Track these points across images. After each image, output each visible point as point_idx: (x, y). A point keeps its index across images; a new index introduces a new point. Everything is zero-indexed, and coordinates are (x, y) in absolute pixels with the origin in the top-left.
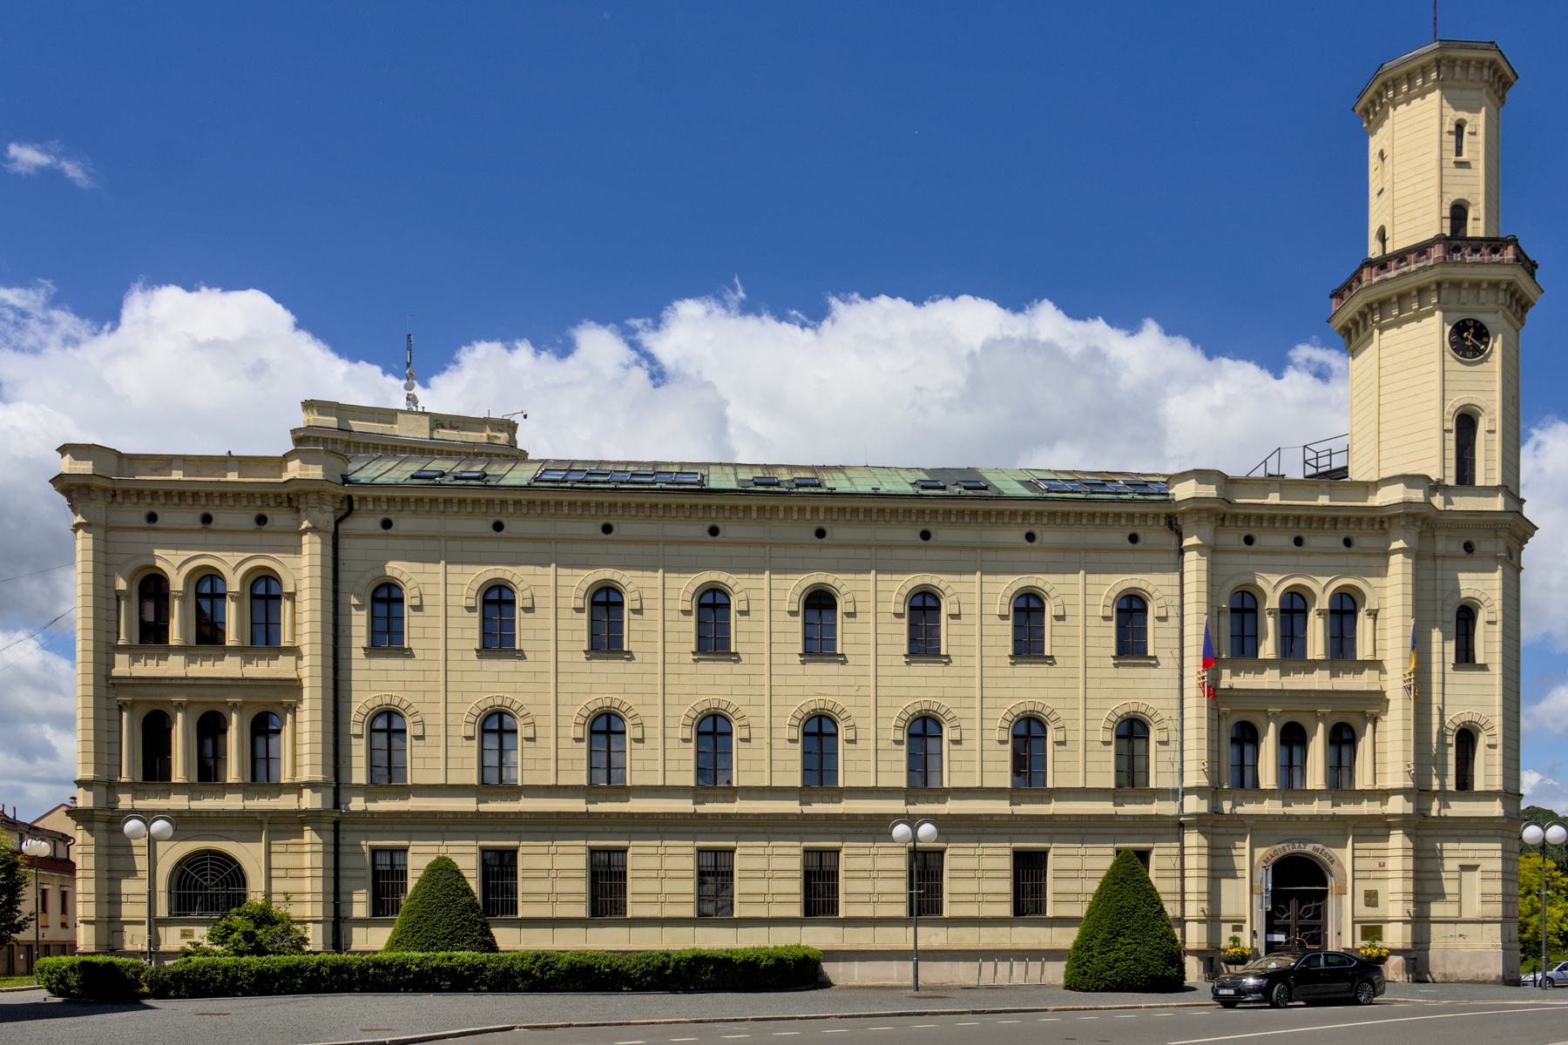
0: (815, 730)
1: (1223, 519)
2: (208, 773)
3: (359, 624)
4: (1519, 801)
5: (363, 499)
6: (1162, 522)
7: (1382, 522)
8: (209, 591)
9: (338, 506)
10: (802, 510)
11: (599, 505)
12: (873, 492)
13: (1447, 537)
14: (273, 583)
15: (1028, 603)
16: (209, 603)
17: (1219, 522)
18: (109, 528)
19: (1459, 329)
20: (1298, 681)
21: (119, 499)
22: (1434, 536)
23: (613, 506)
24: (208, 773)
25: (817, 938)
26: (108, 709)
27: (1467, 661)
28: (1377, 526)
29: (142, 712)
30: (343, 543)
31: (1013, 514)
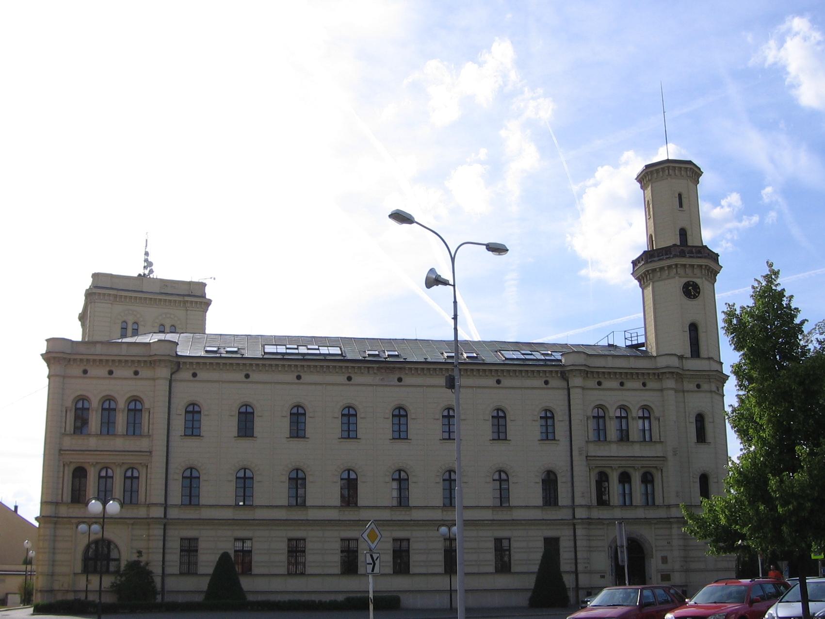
0: (397, 477)
1: (587, 374)
3: (179, 424)
5: (185, 363)
6: (559, 375)
7: (658, 376)
8: (108, 407)
9: (173, 366)
12: (424, 360)
13: (688, 382)
14: (138, 403)
15: (498, 413)
17: (585, 375)
18: (64, 377)
20: (624, 451)
21: (72, 363)
22: (683, 382)
25: (399, 583)
28: (656, 377)
29: (72, 467)
30: (173, 384)
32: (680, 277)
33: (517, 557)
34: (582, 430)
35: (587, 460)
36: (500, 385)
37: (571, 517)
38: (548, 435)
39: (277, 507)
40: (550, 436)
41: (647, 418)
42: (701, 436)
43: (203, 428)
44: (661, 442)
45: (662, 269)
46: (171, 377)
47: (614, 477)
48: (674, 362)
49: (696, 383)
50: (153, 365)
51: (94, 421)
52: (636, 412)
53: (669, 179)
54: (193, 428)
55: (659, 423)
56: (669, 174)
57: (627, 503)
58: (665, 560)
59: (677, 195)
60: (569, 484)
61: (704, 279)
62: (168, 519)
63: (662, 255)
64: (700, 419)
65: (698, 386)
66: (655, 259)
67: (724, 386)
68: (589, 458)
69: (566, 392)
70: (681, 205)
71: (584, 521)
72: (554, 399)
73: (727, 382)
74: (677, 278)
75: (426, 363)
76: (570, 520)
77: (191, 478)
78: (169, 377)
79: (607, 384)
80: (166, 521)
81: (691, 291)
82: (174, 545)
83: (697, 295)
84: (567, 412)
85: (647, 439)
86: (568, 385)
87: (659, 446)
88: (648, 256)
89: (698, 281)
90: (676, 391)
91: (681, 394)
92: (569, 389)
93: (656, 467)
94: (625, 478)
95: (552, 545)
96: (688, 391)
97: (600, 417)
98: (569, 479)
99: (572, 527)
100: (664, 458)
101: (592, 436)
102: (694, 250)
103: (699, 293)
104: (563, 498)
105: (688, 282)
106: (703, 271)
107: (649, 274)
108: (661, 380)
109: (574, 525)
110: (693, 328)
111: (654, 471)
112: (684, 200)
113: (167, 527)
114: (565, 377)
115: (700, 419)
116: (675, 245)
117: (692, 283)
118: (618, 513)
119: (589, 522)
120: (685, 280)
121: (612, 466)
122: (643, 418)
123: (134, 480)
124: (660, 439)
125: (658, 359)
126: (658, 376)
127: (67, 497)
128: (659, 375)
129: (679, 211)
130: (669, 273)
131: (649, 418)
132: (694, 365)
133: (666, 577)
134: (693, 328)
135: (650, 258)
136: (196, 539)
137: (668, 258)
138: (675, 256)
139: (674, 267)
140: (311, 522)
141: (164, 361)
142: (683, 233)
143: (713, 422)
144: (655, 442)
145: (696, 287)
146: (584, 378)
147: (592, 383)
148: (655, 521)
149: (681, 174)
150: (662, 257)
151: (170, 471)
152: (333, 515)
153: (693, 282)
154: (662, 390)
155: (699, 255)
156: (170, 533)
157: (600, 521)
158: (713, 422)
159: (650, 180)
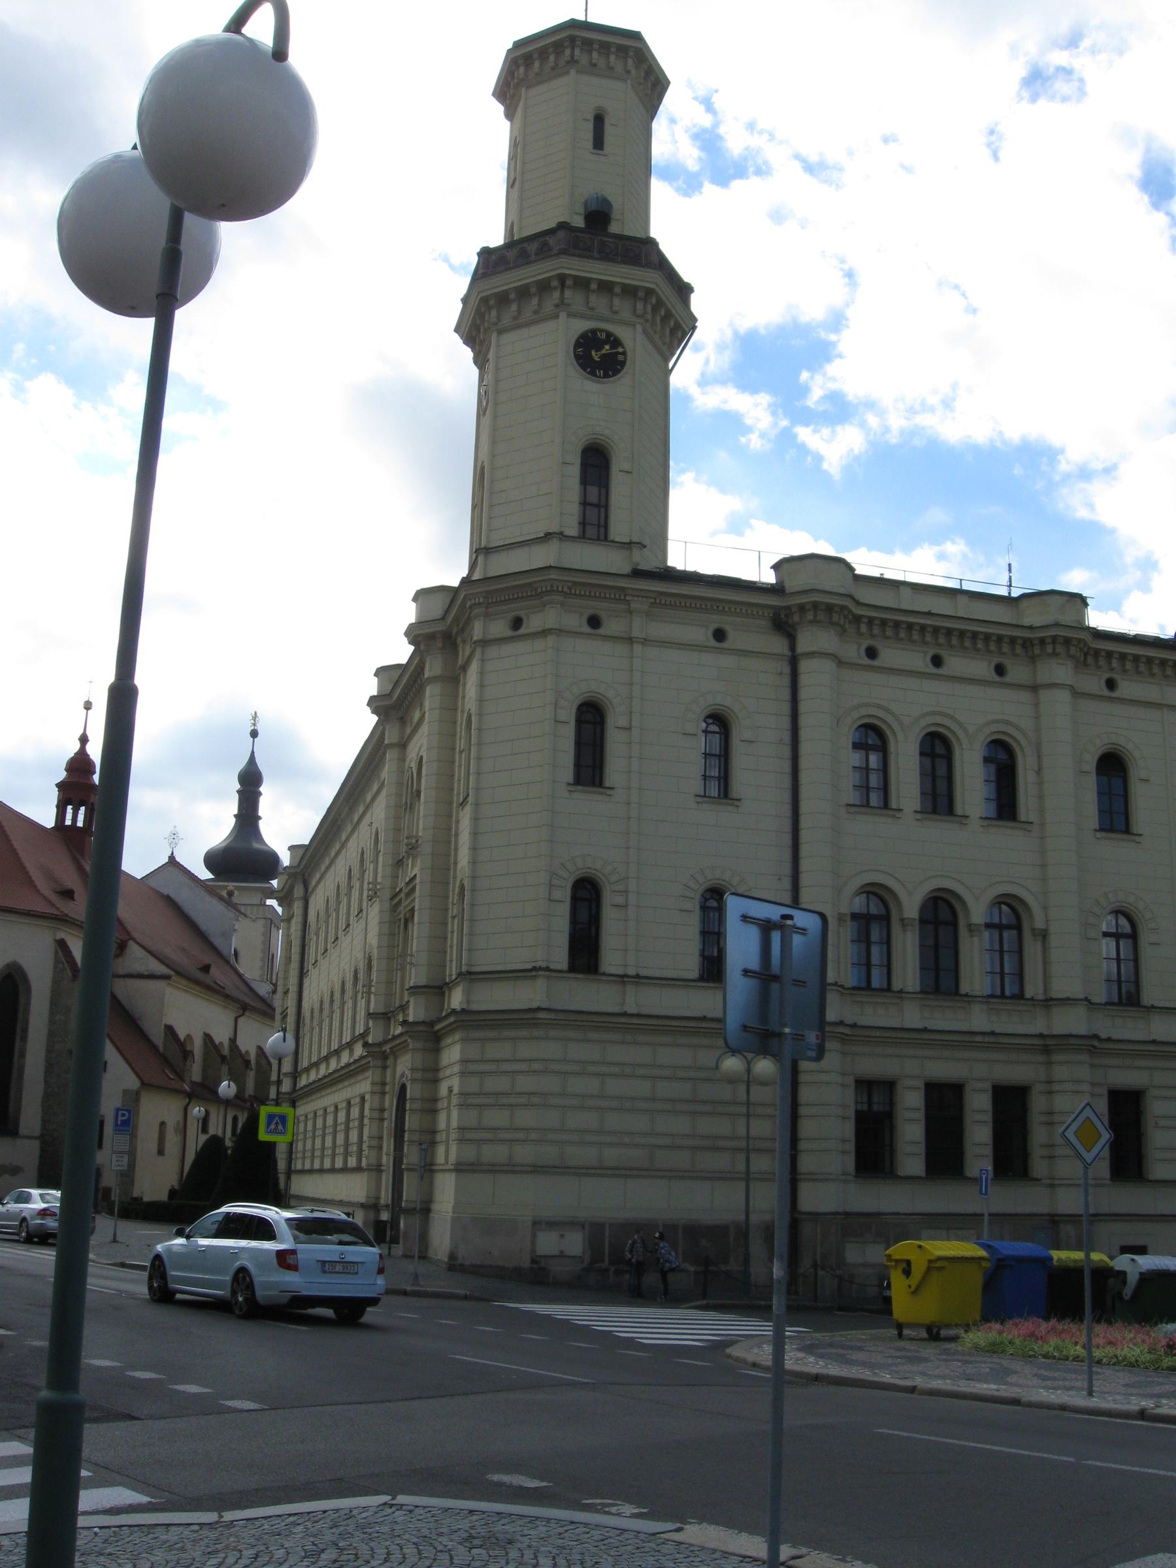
27: (593, 784)
32: (570, 315)
59: (591, 117)
61: (639, 328)
105: (594, 331)
106: (640, 306)
112: (608, 129)
117: (604, 336)
120: (582, 326)
130: (540, 305)
139: (555, 283)
153: (609, 334)
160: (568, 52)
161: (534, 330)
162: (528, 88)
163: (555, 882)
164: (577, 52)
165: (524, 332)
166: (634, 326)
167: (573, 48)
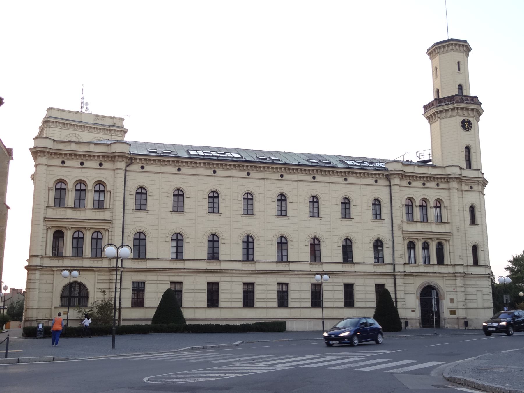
1: (402, 177)
2: (78, 252)
3: (131, 201)
4: (490, 269)
5: (136, 159)
6: (385, 176)
7: (447, 179)
8: (79, 188)
9: (127, 161)
10: (277, 168)
11: (213, 164)
12: (298, 163)
16: (79, 192)
17: (401, 178)
19: (463, 122)
22: (461, 184)
23: (217, 164)
24: (78, 252)
25: (281, 314)
26: (43, 229)
28: (446, 180)
29: (53, 230)
30: (127, 173)
31: (341, 172)
32: (459, 116)
33: (358, 296)
34: (400, 213)
35: (402, 233)
36: (347, 182)
37: (393, 271)
38: (377, 216)
39: (200, 260)
40: (378, 217)
41: (438, 207)
42: (473, 221)
43: (148, 205)
44: (448, 223)
45: (447, 110)
46: (126, 168)
47: (419, 245)
48: (457, 171)
49: (471, 185)
50: (113, 160)
51: (70, 198)
52: (432, 203)
53: (452, 52)
54: (141, 204)
55: (447, 211)
56: (452, 49)
57: (427, 262)
58: (452, 300)
59: (457, 63)
60: (391, 249)
61: (474, 118)
62: (124, 268)
63: (448, 102)
64: (472, 209)
65: (471, 187)
66: (442, 104)
67: (484, 188)
68: (403, 232)
69: (388, 188)
70: (459, 70)
71: (402, 273)
72: (381, 193)
73: (486, 186)
74: (458, 116)
75: (299, 165)
76: (392, 272)
77: (140, 239)
78: (125, 169)
79: (414, 184)
80: (122, 269)
81: (467, 125)
82: (128, 287)
83: (470, 128)
84: (389, 202)
85: (439, 220)
86: (390, 184)
87: (447, 225)
88: (438, 101)
89: (471, 119)
90: (458, 190)
91: (460, 192)
92: (390, 186)
93: (445, 240)
94: (426, 247)
95: (380, 289)
96: (465, 191)
97: (410, 204)
98: (391, 246)
99: (393, 277)
100: (450, 234)
101: (405, 218)
102: (469, 99)
103: (471, 127)
104: (388, 258)
105: (465, 119)
107: (438, 114)
108: (448, 182)
109: (395, 276)
110: (468, 149)
111: (443, 242)
112: (461, 66)
113: (123, 273)
114: (388, 178)
115: (472, 209)
116: (457, 95)
118: (423, 269)
119: (404, 274)
120: (463, 118)
121: (418, 237)
122: (436, 207)
123: (98, 240)
124: (448, 221)
125: (447, 168)
126: (447, 179)
127: (49, 253)
128: (447, 179)
129: (458, 73)
131: (440, 207)
132: (468, 173)
133: (453, 312)
134: (468, 149)
135: (439, 104)
136: (143, 282)
137: (451, 103)
138: (457, 102)
139: (456, 109)
140: (223, 271)
141: (122, 157)
142: (460, 87)
143: (481, 211)
144: (445, 223)
145: (469, 123)
146: (400, 179)
147: (405, 183)
148: (446, 275)
149: (460, 49)
150: (447, 103)
151: (125, 234)
152: (238, 266)
153: (468, 120)
154: (449, 189)
155: (472, 102)
156: (124, 278)
157: (411, 274)
158: (481, 211)
159: (439, 53)
160: (451, 47)
161: (450, 119)
162: (439, 55)
163: (469, 246)
164: (453, 47)
165: (447, 120)
166: (473, 117)
167: (452, 46)
